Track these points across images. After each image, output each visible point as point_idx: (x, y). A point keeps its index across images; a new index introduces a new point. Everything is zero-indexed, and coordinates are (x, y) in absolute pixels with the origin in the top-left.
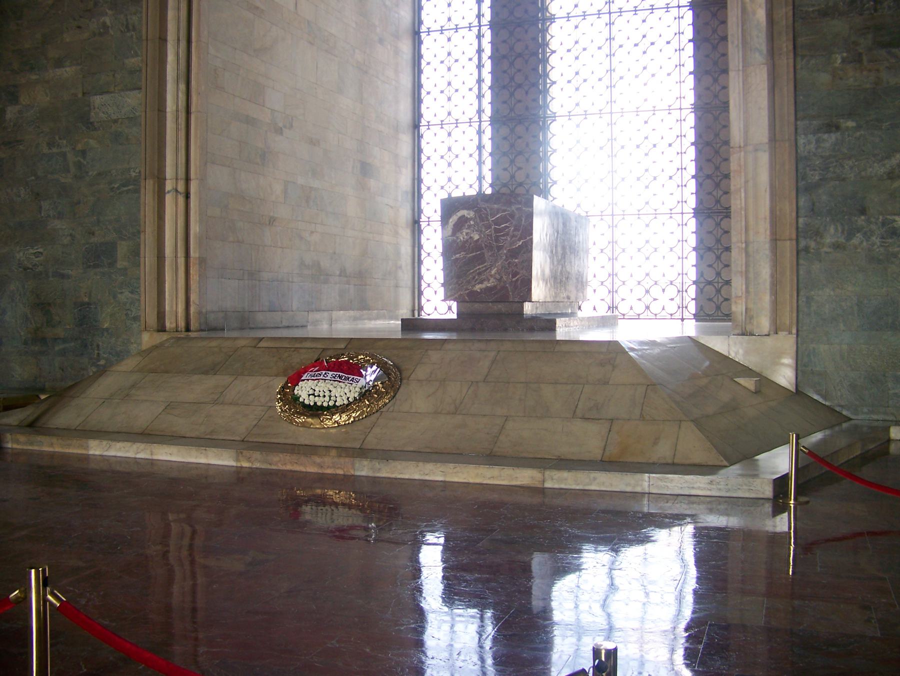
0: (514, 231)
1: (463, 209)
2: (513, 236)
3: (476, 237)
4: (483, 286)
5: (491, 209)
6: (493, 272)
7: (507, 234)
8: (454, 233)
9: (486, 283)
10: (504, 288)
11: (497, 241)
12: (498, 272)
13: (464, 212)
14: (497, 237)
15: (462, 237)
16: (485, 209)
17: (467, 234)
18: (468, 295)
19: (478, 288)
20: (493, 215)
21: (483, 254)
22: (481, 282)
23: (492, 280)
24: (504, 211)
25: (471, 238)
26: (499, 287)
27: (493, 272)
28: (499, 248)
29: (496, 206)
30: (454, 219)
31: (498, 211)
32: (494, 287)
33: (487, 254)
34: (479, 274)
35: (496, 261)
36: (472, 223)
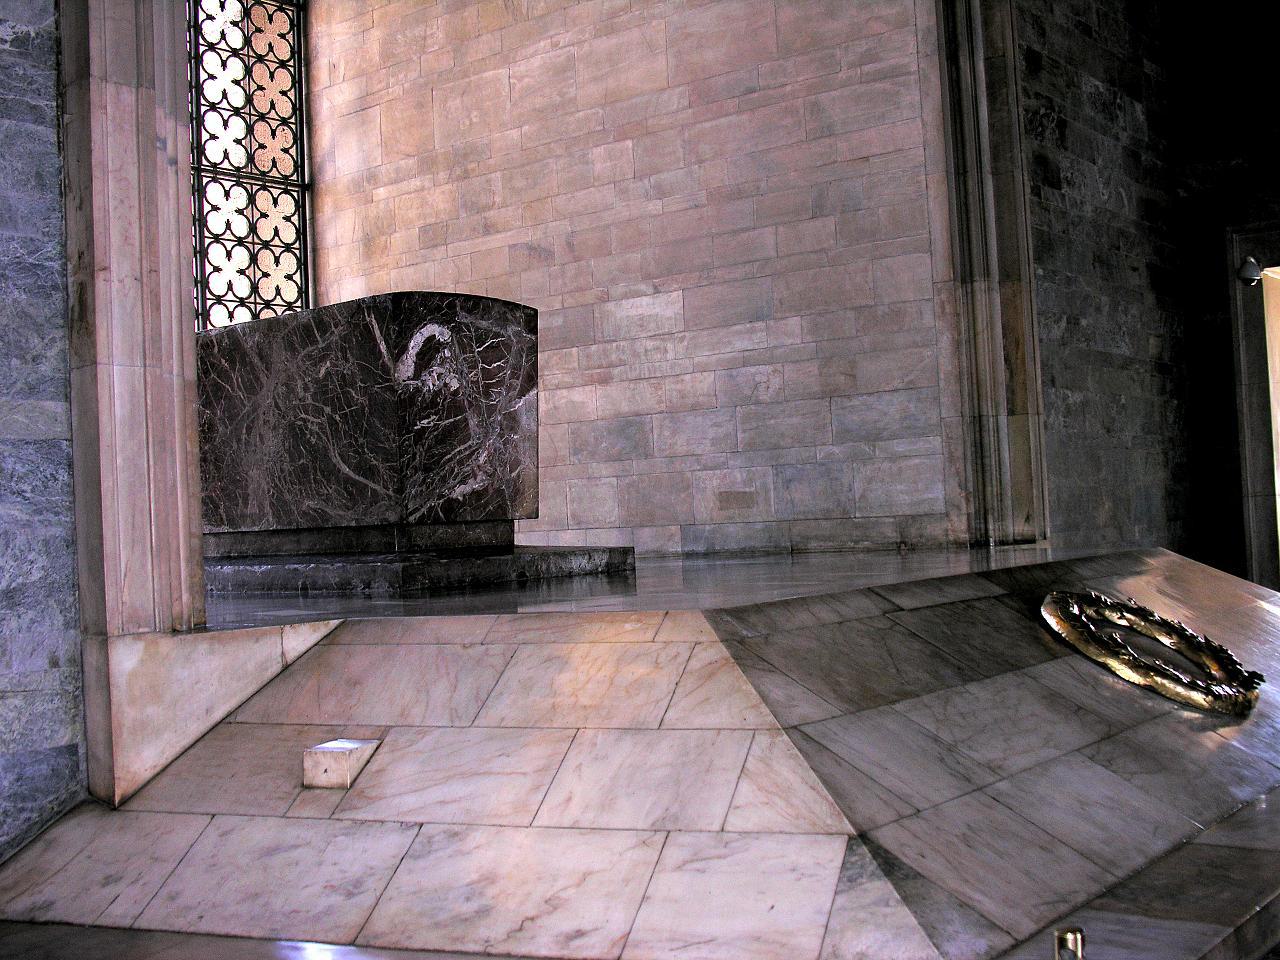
0: (514, 375)
1: (431, 321)
2: (508, 390)
3: (455, 385)
4: (466, 489)
5: (477, 329)
6: (482, 459)
7: (499, 384)
8: (417, 376)
9: (471, 481)
10: (499, 492)
11: (487, 395)
12: (490, 461)
13: (432, 329)
14: (488, 387)
15: (431, 382)
16: (467, 326)
17: (439, 376)
18: (443, 508)
19: (459, 492)
20: (480, 341)
21: (466, 420)
22: (463, 482)
23: (481, 476)
24: (497, 335)
25: (446, 385)
26: (491, 491)
27: (482, 459)
28: (491, 410)
29: (484, 324)
30: (416, 342)
31: (487, 332)
32: (486, 490)
33: (473, 422)
34: (461, 463)
35: (486, 436)
36: (447, 353)
